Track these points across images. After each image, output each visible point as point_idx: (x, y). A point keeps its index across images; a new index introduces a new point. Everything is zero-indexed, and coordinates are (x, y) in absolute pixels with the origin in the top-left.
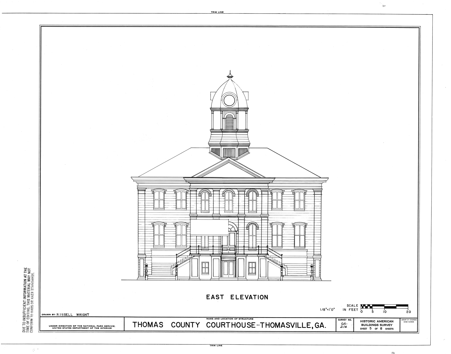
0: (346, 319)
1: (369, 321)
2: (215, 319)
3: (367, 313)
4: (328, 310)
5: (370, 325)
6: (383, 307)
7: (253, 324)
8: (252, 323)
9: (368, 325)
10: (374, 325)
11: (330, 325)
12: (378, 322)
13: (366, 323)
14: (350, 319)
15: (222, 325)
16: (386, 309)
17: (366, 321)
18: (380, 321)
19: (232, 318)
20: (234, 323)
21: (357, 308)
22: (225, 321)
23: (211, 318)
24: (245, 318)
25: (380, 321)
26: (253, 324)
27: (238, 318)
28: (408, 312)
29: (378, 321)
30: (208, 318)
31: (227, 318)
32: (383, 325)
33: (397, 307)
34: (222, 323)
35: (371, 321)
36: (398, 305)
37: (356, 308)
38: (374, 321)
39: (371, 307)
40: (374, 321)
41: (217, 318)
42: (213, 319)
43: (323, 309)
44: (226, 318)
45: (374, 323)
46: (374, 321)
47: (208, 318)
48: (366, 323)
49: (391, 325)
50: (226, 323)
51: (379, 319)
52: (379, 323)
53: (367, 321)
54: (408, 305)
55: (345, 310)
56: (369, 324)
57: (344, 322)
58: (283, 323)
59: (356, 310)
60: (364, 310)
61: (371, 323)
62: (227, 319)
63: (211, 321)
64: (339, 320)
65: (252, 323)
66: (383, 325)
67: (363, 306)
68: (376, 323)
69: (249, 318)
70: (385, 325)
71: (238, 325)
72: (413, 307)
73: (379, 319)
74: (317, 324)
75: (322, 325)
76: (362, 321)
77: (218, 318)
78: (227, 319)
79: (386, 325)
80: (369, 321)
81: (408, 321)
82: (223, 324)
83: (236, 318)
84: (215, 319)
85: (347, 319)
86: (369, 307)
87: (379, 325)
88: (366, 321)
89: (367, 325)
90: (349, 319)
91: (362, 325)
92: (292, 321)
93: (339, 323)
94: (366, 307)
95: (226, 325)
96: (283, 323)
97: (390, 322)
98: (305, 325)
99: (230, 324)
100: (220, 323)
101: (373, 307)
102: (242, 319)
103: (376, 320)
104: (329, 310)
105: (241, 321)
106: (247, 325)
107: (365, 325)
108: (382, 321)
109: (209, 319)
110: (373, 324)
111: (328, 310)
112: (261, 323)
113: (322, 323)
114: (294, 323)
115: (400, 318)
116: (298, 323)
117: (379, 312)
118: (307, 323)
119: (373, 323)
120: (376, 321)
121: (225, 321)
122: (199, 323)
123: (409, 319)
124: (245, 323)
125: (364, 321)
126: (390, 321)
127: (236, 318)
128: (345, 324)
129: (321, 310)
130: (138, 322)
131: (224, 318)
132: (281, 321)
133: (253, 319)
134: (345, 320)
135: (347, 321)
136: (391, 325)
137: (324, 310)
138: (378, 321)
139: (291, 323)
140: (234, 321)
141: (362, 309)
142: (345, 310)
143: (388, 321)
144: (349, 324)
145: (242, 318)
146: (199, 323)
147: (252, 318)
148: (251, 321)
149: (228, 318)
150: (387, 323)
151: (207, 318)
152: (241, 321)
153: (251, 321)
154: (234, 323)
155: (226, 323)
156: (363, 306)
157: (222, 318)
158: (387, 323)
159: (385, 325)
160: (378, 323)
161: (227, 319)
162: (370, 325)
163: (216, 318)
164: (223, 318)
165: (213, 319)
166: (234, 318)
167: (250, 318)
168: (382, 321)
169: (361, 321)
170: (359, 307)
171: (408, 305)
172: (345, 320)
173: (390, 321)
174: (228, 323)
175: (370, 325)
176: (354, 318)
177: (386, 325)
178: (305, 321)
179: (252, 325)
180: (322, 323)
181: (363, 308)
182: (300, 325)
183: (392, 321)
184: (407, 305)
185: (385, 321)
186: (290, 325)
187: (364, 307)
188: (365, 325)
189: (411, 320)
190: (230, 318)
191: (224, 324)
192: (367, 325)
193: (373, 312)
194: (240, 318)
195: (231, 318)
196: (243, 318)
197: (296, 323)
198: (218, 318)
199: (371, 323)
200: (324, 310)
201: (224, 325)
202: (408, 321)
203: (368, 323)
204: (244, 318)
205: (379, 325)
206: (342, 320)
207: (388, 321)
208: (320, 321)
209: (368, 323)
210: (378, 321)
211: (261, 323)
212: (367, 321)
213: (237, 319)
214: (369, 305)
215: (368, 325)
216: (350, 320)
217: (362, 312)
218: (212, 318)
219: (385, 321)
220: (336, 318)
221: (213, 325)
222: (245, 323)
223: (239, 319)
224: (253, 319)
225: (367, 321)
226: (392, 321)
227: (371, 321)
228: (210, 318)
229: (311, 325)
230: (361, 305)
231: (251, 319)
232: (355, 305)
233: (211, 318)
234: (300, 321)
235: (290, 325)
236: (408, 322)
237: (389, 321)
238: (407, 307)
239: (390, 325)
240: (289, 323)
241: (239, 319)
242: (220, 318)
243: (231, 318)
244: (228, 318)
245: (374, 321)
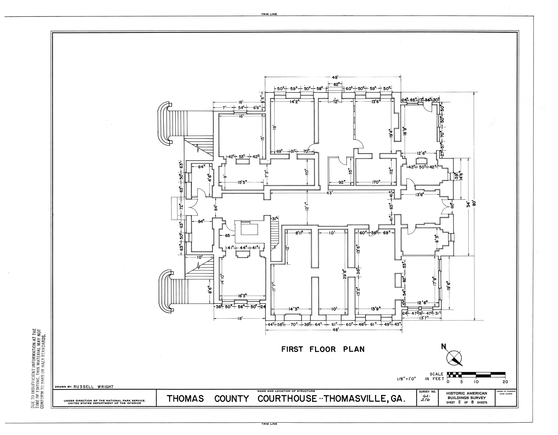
0: (429, 390)
1: (457, 393)
2: (268, 391)
3: (455, 382)
4: (407, 379)
5: (458, 398)
6: (475, 376)
7: (314, 397)
8: (313, 396)
9: (456, 398)
10: (463, 398)
11: (409, 398)
12: (468, 394)
13: (453, 395)
14: (433, 390)
15: (276, 398)
16: (478, 379)
17: (453, 393)
18: (470, 393)
19: (289, 390)
20: (290, 397)
21: (443, 376)
22: (280, 394)
23: (264, 390)
24: (305, 390)
25: (470, 393)
26: (314, 397)
27: (296, 390)
28: (505, 382)
29: (468, 392)
30: (260, 390)
31: (283, 390)
32: (474, 398)
33: (492, 376)
34: (276, 396)
35: (460, 393)
36: (493, 373)
37: (441, 376)
38: (463, 393)
39: (460, 376)
40: (463, 393)
41: (270, 390)
42: (265, 391)
43: (400, 379)
44: (281, 390)
45: (464, 396)
46: (464, 393)
47: (259, 390)
48: (453, 395)
49: (485, 398)
50: (282, 396)
51: (469, 391)
52: (470, 396)
53: (454, 393)
54: (505, 372)
55: (428, 379)
56: (457, 397)
57: (426, 394)
58: (352, 396)
59: (441, 379)
60: (452, 379)
61: (459, 395)
62: (283, 391)
63: (263, 394)
64: (420, 392)
65: (313, 396)
66: (474, 398)
67: (449, 374)
68: (466, 395)
69: (310, 390)
70: (477, 398)
71: (297, 398)
72: (511, 376)
73: (469, 391)
74: (394, 397)
75: (399, 399)
76: (449, 393)
77: (271, 390)
78: (282, 391)
79: (478, 398)
80: (457, 393)
81: (505, 393)
82: (277, 398)
83: (294, 390)
84: (268, 391)
85: (430, 391)
86: (457, 376)
87: (470, 398)
88: (453, 393)
89: (454, 398)
90: (432, 390)
91: (449, 398)
92: (363, 393)
93: (420, 395)
94: (454, 376)
95: (282, 398)
96: (352, 396)
97: (483, 394)
98: (379, 398)
99: (286, 398)
100: (274, 396)
101: (463, 376)
102: (302, 391)
103: (466, 391)
104: (408, 379)
105: (299, 394)
106: (306, 399)
107: (452, 398)
108: (473, 393)
109: (261, 391)
110: (462, 397)
111: (407, 379)
112: (324, 396)
113: (399, 396)
114: (366, 396)
115: (495, 389)
116: (370, 396)
117: (469, 382)
118: (382, 396)
119: (462, 396)
120: (466, 393)
121: (280, 394)
122: (248, 396)
123: (507, 390)
124: (304, 396)
125: (452, 393)
126: (483, 392)
127: (294, 390)
128: (427, 396)
129: (398, 379)
130: (174, 396)
131: (279, 390)
132: (349, 393)
133: (314, 391)
134: (428, 392)
135: (430, 393)
136: (485, 398)
137: (402, 379)
138: (468, 393)
139: (361, 396)
140: (290, 394)
141: (449, 379)
142: (428, 379)
143: (481, 393)
144: (433, 397)
145: (301, 390)
146: (248, 396)
147: (313, 390)
148: (311, 394)
149: (284, 391)
150: (479, 396)
151: (259, 390)
152: (299, 394)
153: (311, 394)
154: (290, 397)
155: (282, 396)
156: (449, 374)
157: (276, 390)
158: (479, 396)
159: (477, 398)
160: (468, 395)
161: (283, 391)
162: (458, 398)
163: (269, 390)
164: (278, 390)
165: (265, 391)
166: (291, 390)
167: (311, 390)
168: (473, 393)
169: (447, 393)
170: (445, 375)
171: (505, 372)
172: (428, 392)
173: (483, 392)
174: (284, 396)
175: (458, 398)
176: (438, 389)
177: (478, 398)
178: (379, 394)
179: (313, 398)
180: (399, 396)
181: (450, 377)
182: (372, 398)
183: (485, 393)
184: (504, 373)
185: (477, 393)
186: (360, 398)
187: (452, 376)
188: (452, 398)
189: (509, 391)
190: (286, 390)
191: (278, 397)
192: (454, 398)
193: (462, 382)
194: (299, 390)
195: (288, 390)
196: (303, 390)
197: (367, 396)
198: (272, 390)
199: (459, 395)
200: (402, 379)
201: (279, 398)
202: (505, 393)
203: (456, 396)
204: (304, 390)
205: (470, 398)
206: (423, 391)
207: (481, 393)
208: (397, 393)
209: (456, 396)
210: (468, 392)
211: (324, 396)
212: (455, 393)
213: (295, 391)
214: (457, 373)
215: (456, 398)
216: (434, 392)
217: (448, 382)
218: (264, 390)
219: (477, 393)
220: (417, 389)
221: (266, 398)
222: (304, 396)
223: (298, 391)
224: (314, 391)
225: (455, 393)
226: (485, 393)
227: (460, 393)
228: (261, 390)
229: (386, 398)
230: (448, 373)
231: (312, 391)
232: (440, 374)
233: (263, 390)
234: (372, 394)
235: (360, 398)
236: (505, 394)
237: (482, 393)
238: (504, 376)
239: (483, 398)
240: (359, 396)
241: (298, 391)
242: (274, 390)
243: (288, 390)
244: (284, 391)
245: (464, 393)
